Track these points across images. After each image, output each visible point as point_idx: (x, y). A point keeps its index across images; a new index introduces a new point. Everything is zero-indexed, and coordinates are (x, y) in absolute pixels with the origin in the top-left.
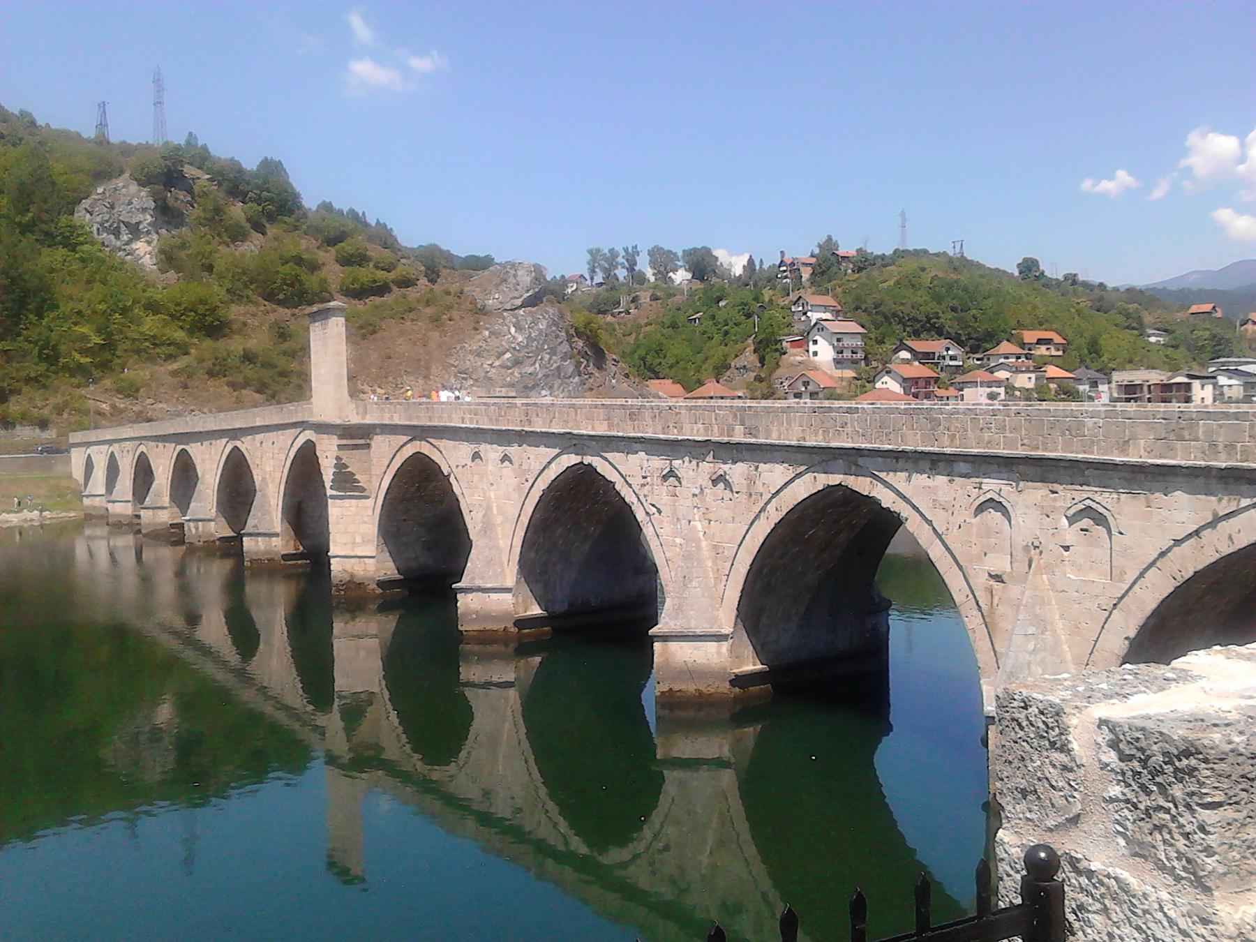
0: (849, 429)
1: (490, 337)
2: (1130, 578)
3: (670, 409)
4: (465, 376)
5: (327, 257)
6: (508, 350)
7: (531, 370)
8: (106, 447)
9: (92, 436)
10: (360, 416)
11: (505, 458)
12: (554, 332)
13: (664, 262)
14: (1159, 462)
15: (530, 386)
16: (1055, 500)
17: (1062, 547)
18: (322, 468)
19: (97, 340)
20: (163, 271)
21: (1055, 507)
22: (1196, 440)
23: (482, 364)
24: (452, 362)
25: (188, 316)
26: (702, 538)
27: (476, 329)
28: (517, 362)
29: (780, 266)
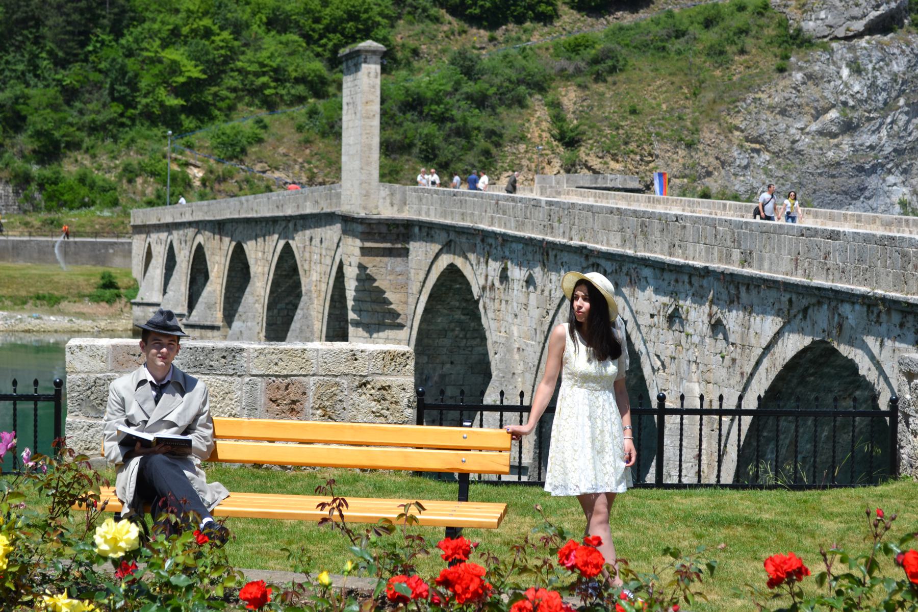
1: (804, 83)
3: (677, 220)
4: (757, 146)
6: (834, 106)
7: (868, 139)
8: (163, 235)
10: (396, 208)
11: (530, 281)
15: (867, 167)
18: (346, 279)
19: (194, 71)
23: (788, 127)
24: (738, 121)
25: (330, 40)
27: (781, 70)
28: (849, 127)
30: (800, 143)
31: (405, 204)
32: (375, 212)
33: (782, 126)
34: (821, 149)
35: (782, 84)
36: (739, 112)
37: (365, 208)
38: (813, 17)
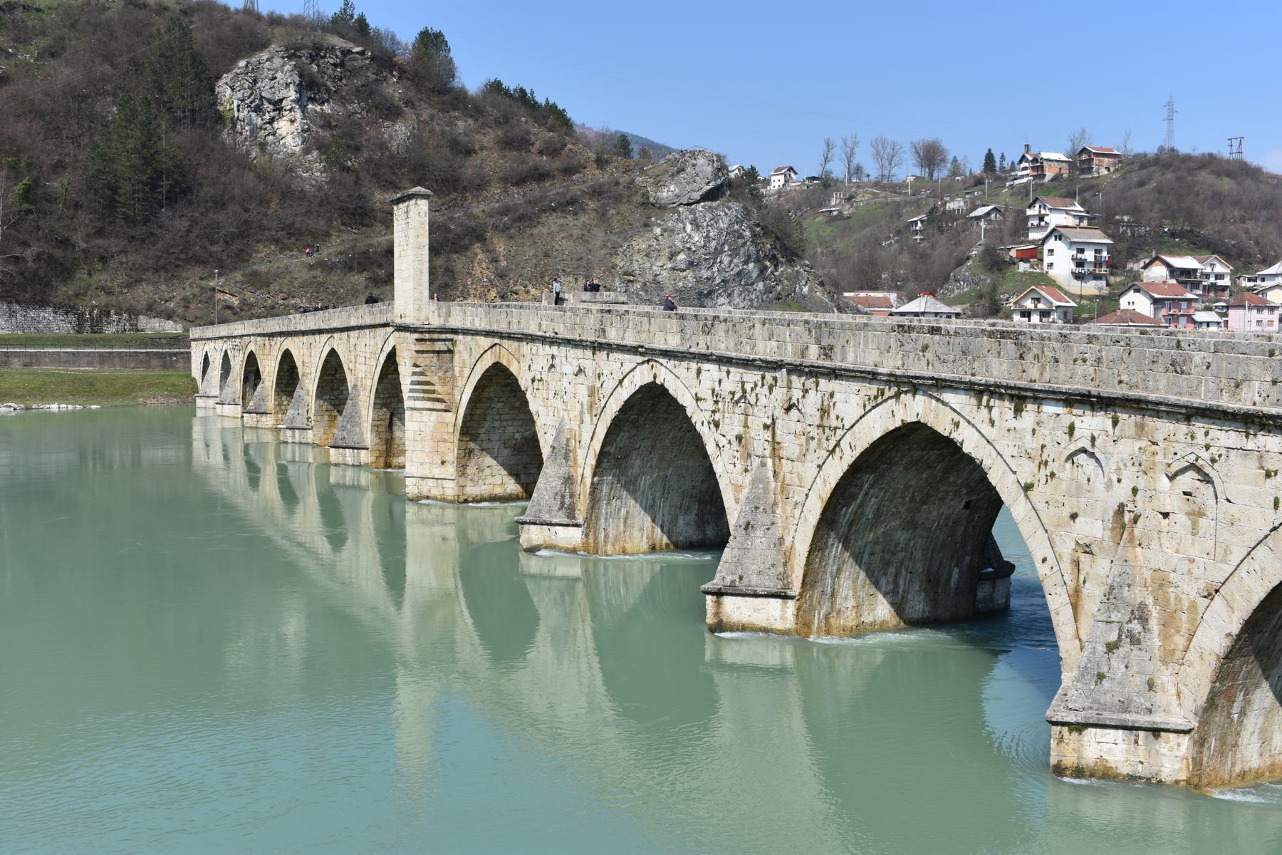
1: (662, 235)
2: (1235, 559)
4: (632, 278)
7: (705, 274)
8: (219, 343)
9: (210, 331)
10: (442, 319)
12: (738, 231)
13: (887, 155)
15: (705, 292)
17: (1161, 513)
18: (401, 376)
26: (772, 479)
27: (646, 225)
28: (691, 265)
29: (1021, 162)
30: (660, 277)
31: (449, 316)
32: (427, 323)
33: (648, 265)
34: (675, 280)
35: (647, 235)
36: (618, 255)
37: (418, 320)
38: (666, 190)
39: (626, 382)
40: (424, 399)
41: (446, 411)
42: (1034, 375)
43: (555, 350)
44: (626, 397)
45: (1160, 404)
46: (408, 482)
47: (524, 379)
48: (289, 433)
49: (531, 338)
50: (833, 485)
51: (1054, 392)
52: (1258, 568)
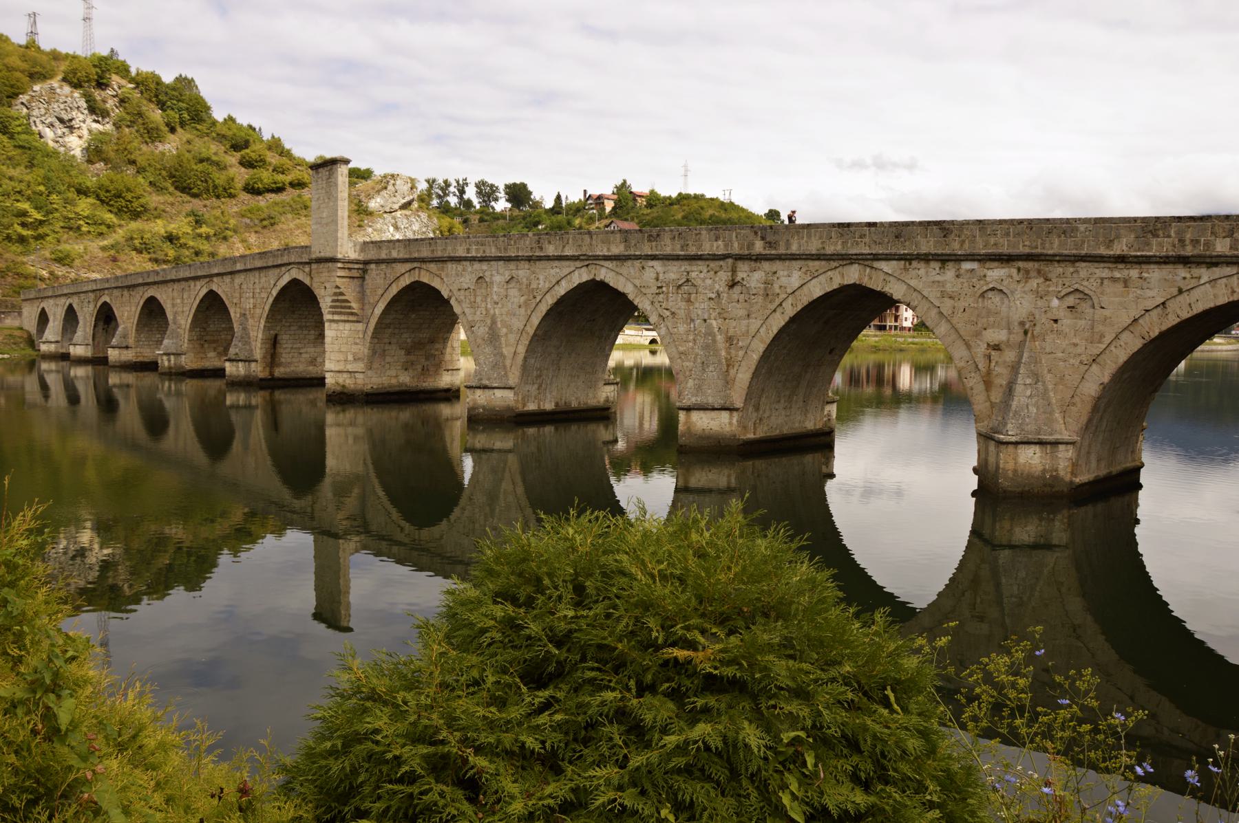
0: (867, 240)
2: (1107, 340)
5: (232, 159)
14: (1139, 254)
16: (1049, 286)
20: (90, 162)
21: (1048, 292)
22: (1169, 236)
27: (359, 226)
39: (563, 283)
40: (340, 313)
41: (358, 322)
42: (955, 247)
43: (485, 266)
44: (563, 292)
45: (1056, 255)
46: (327, 375)
47: (448, 290)
48: (165, 358)
49: (459, 260)
50: (775, 332)
51: (973, 255)
52: (1122, 344)
